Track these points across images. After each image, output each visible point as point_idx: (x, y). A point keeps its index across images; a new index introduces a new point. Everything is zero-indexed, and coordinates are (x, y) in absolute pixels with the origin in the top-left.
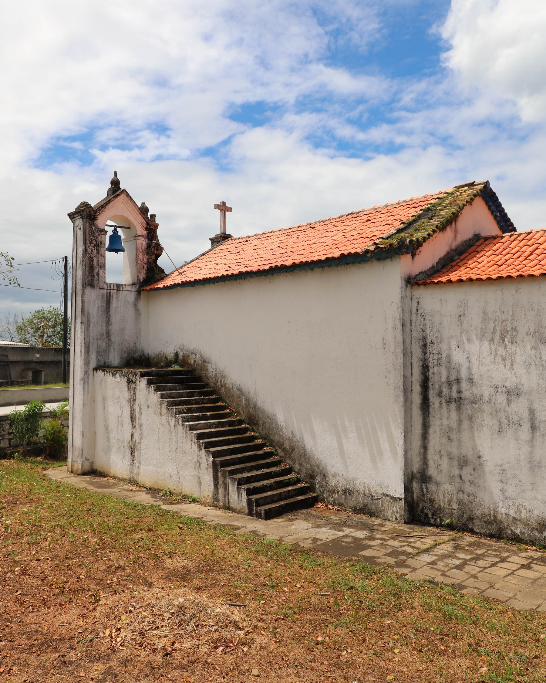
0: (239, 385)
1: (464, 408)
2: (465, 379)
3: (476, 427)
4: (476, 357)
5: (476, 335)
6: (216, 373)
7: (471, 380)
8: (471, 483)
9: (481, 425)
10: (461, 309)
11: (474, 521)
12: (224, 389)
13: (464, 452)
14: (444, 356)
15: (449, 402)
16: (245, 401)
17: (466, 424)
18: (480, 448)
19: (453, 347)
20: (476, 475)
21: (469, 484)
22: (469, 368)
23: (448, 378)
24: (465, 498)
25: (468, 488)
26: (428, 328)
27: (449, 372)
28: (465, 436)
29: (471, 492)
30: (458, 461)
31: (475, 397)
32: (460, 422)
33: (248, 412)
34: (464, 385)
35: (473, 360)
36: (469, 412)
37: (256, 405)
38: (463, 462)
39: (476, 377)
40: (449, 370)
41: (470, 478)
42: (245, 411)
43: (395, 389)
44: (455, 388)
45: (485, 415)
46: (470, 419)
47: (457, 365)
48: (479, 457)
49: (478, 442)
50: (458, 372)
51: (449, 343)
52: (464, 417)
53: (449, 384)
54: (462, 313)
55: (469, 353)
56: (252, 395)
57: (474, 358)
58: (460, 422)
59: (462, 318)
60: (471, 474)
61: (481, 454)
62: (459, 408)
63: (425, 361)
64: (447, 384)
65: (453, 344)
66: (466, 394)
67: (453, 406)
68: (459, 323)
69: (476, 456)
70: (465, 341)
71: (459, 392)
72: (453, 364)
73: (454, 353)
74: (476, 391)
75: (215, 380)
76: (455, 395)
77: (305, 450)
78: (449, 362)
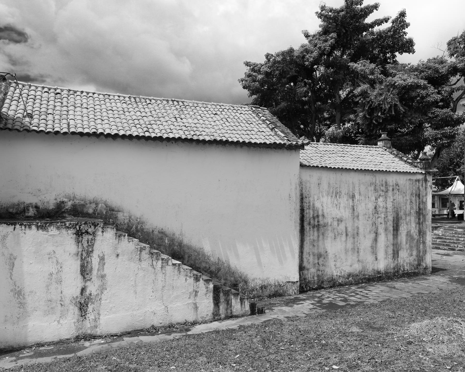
0: (162, 229)
1: (320, 229)
2: (320, 215)
3: (325, 238)
4: (326, 204)
5: (326, 194)
6: (130, 221)
7: (323, 215)
8: (323, 265)
9: (327, 237)
10: (319, 181)
11: (324, 283)
12: (141, 233)
13: (320, 251)
14: (311, 204)
15: (314, 227)
16: (168, 241)
17: (321, 237)
18: (327, 248)
19: (316, 199)
20: (325, 260)
21: (322, 266)
22: (323, 210)
23: (313, 215)
24: (320, 273)
25: (321, 268)
26: (304, 189)
27: (314, 212)
28: (321, 243)
29: (322, 270)
30: (317, 256)
31: (325, 223)
32: (318, 236)
33: (172, 250)
34: (321, 218)
35: (324, 206)
36: (323, 231)
37: (182, 243)
38: (319, 256)
39: (325, 214)
40: (314, 211)
41: (322, 263)
42: (167, 249)
43: (295, 222)
44: (316, 220)
45: (329, 232)
46: (323, 235)
47: (317, 208)
48: (326, 252)
49: (326, 245)
50: (318, 212)
51: (314, 197)
52: (320, 234)
53: (314, 218)
54: (320, 183)
55: (323, 202)
56: (178, 236)
57: (324, 205)
58: (318, 236)
59: (320, 185)
60: (323, 261)
61: (327, 250)
62: (318, 230)
63: (302, 207)
64: (313, 218)
65: (316, 197)
66: (321, 223)
67: (316, 229)
68: (318, 188)
69: (325, 252)
70: (321, 196)
71: (318, 222)
72: (316, 208)
73: (316, 202)
74: (326, 221)
75: (128, 226)
76: (316, 223)
77: (229, 267)
78: (314, 207)
